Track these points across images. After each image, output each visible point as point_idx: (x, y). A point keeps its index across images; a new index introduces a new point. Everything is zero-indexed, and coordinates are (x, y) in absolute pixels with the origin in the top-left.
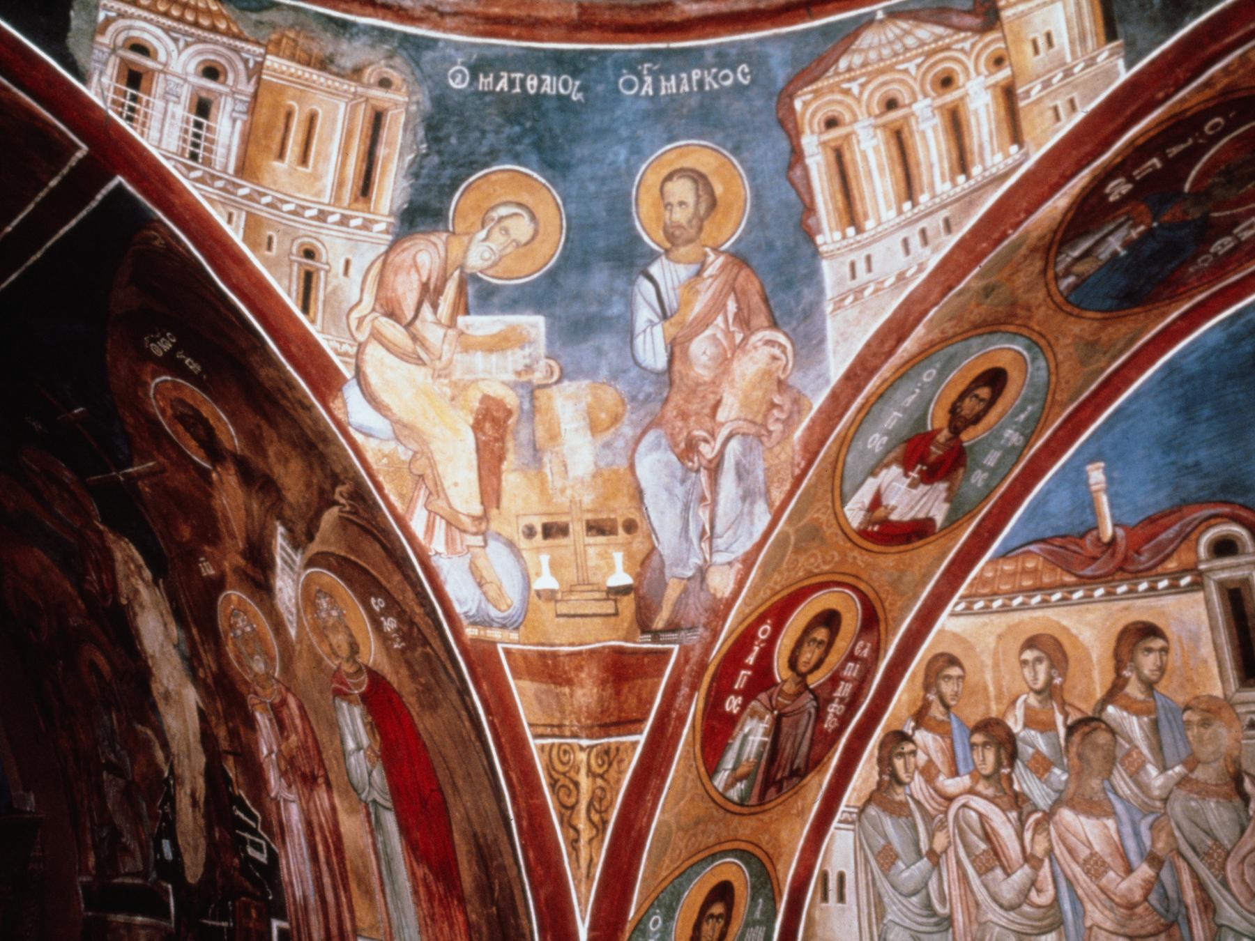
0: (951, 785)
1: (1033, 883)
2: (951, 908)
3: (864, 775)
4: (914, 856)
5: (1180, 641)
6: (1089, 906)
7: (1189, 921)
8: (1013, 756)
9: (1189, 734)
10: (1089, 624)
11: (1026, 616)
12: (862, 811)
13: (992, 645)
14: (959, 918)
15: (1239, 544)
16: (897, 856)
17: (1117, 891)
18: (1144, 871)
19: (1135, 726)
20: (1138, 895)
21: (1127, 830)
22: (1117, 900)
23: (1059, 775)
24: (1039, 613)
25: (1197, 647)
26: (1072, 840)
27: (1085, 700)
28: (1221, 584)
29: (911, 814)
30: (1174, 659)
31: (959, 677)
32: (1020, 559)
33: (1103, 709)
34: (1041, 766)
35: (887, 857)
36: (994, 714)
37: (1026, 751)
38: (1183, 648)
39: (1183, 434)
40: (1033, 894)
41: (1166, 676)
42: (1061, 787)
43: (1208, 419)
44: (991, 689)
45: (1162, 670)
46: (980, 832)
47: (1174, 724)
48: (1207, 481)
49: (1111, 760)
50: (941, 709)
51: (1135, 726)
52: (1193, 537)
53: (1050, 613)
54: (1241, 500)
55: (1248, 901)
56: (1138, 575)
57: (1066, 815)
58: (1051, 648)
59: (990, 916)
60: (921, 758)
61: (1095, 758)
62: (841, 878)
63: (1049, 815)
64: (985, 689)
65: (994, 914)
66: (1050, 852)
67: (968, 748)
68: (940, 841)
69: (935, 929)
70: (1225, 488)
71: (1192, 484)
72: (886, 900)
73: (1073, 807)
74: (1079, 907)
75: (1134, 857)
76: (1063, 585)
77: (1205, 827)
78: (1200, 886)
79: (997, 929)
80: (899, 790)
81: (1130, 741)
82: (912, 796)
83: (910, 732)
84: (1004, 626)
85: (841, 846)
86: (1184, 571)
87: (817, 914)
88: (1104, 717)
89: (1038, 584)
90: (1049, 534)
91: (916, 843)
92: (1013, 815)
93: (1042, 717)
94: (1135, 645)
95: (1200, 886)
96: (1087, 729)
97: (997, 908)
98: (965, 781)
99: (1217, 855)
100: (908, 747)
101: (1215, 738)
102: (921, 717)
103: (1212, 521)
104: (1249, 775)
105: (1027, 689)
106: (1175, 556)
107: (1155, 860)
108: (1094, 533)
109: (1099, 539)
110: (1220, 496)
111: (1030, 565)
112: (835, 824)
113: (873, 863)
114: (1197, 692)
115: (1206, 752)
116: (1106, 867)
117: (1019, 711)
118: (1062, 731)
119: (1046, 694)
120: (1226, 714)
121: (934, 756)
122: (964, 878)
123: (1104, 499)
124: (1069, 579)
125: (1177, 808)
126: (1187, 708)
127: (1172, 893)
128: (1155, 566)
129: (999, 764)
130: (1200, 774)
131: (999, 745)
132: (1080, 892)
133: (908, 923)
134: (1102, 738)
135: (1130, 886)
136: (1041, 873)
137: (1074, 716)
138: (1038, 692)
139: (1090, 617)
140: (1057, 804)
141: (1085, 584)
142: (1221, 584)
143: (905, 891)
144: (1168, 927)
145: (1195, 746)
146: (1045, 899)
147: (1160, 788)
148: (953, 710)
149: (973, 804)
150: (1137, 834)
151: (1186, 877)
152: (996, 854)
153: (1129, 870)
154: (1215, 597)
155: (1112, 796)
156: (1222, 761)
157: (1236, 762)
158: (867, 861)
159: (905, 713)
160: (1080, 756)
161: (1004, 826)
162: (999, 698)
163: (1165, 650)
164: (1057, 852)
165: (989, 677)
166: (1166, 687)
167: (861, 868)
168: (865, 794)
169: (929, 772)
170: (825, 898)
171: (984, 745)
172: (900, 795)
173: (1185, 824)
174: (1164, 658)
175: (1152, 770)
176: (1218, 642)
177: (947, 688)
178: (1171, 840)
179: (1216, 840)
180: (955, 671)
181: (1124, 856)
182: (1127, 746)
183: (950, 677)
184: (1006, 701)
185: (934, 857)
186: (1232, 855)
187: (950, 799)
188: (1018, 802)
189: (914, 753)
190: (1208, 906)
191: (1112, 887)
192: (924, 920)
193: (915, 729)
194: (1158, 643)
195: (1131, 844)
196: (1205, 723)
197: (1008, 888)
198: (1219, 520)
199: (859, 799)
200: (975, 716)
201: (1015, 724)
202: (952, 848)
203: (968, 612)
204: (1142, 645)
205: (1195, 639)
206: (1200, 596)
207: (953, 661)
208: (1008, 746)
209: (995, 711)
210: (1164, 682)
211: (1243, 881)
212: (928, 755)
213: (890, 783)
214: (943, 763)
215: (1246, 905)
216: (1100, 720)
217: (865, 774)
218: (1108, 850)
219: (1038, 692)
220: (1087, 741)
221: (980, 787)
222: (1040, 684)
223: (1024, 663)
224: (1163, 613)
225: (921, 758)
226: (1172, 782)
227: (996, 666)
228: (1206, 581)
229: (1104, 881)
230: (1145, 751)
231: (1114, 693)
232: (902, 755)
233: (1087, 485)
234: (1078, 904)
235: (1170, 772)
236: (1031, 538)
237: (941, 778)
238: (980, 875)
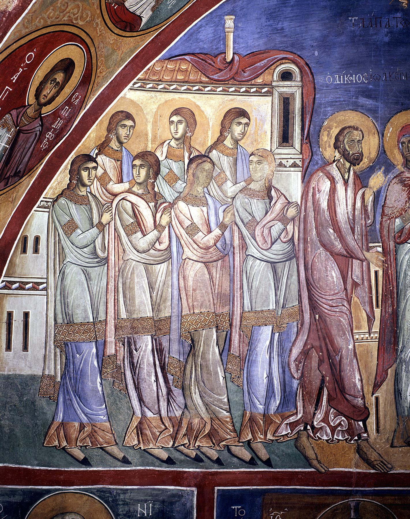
0: (117, 188)
1: (158, 239)
2: (108, 253)
3: (59, 180)
4: (88, 226)
5: (256, 119)
6: (186, 249)
7: (234, 254)
8: (157, 173)
9: (251, 167)
10: (211, 106)
11: (177, 96)
12: (56, 200)
13: (155, 110)
14: (112, 258)
15: (293, 75)
16: (77, 227)
17: (202, 242)
18: (217, 232)
19: (225, 162)
20: (212, 243)
21: (212, 212)
22: (201, 246)
23: (180, 185)
24: (184, 96)
25: (263, 125)
26: (182, 217)
27: (203, 146)
28: (281, 94)
29: (88, 204)
30: (251, 129)
31: (131, 126)
32: (179, 62)
33: (210, 151)
34: (172, 179)
35: (71, 227)
36: (149, 150)
37: (164, 171)
38: (256, 124)
39: (279, 11)
40: (157, 245)
41: (245, 137)
42: (181, 191)
43: (292, 6)
44: (150, 135)
45: (244, 134)
46: (131, 213)
47: (244, 162)
48: (285, 39)
49: (210, 177)
50: (117, 144)
51: (225, 162)
52: (273, 67)
53: (190, 96)
54: (299, 53)
55: (262, 245)
56: (241, 83)
57: (181, 205)
58: (187, 116)
59: (131, 257)
60: (100, 171)
61: (202, 176)
62: (37, 239)
63: (172, 205)
64: (147, 135)
65: (132, 255)
66: (170, 224)
67: (130, 167)
68: (106, 218)
69: (97, 265)
70: (292, 45)
71: (278, 39)
72: (67, 251)
73: (185, 200)
74: (181, 250)
75: (213, 225)
76: (201, 82)
77: (250, 211)
78: (242, 237)
79: (134, 262)
80: (83, 189)
81: (222, 169)
82: (91, 193)
83: (94, 156)
84: (163, 101)
85: (38, 222)
86: (265, 85)
87: (18, 261)
88: (210, 156)
89: (186, 79)
90: (197, 51)
91: (91, 219)
92: (152, 204)
93: (177, 152)
94: (234, 119)
95: (242, 237)
96: (200, 161)
97: (136, 252)
98: (126, 186)
99: (252, 224)
100: (92, 165)
101: (262, 169)
102: (102, 148)
103: (284, 61)
104: (274, 187)
105: (171, 138)
106: (262, 76)
107: (223, 227)
108: (223, 55)
109: (225, 59)
110: (289, 49)
111: (184, 67)
112: (35, 208)
113: (61, 231)
114: (259, 147)
115: (257, 176)
116: (198, 230)
117: (165, 149)
118: (187, 161)
119: (181, 141)
120: (270, 158)
121: (108, 171)
122: (118, 237)
123: (231, 36)
124: (204, 79)
125: (238, 203)
126: (252, 154)
127: (228, 242)
128: (251, 80)
129: (148, 176)
130: (252, 186)
131: (150, 167)
132: (182, 242)
133: (80, 262)
134: (207, 166)
135: (210, 239)
136: (163, 234)
137: (195, 154)
138: (177, 139)
139: (212, 102)
140: (177, 199)
141: (212, 83)
142: (281, 94)
143: (80, 245)
144: (222, 258)
145: (252, 172)
146: (163, 246)
147: (231, 192)
148: (123, 145)
149: (128, 198)
150: (217, 214)
151: (236, 234)
152: (139, 224)
153: (210, 231)
154: (276, 101)
155: (207, 195)
156: (264, 180)
157: (270, 181)
158: (56, 228)
159: (92, 145)
160: (194, 175)
161: (145, 211)
162: (154, 140)
163: (247, 124)
164: (173, 223)
165: (149, 128)
166: (244, 143)
167: (52, 234)
168: (58, 191)
169: (104, 180)
170: (24, 251)
171: (141, 166)
172: (83, 191)
173: (241, 210)
174: (246, 128)
175: (229, 184)
176: (274, 123)
177: (123, 132)
178: (233, 216)
179: (254, 217)
180: (129, 123)
181: (208, 225)
182: (219, 171)
183: (125, 126)
184: (157, 143)
185: (101, 227)
186: (260, 224)
187: (116, 195)
188: (155, 198)
189: (95, 168)
190: (244, 246)
191: (200, 240)
192: (90, 260)
193: (97, 155)
194: (244, 120)
195: (213, 219)
196: (259, 162)
197: (143, 242)
198: (287, 61)
199: (54, 194)
200: (136, 148)
201: (161, 155)
202: (113, 222)
203: (142, 88)
204: (237, 120)
205: (263, 121)
206: (270, 98)
207: (129, 116)
208: (155, 167)
209: (150, 148)
210: (243, 141)
211: (262, 235)
212: (105, 170)
213: (77, 185)
214: (114, 175)
215: (261, 246)
216: (208, 157)
217: (61, 179)
218: (200, 222)
219: (177, 139)
220: (199, 167)
221: (135, 189)
222: (178, 136)
223: (172, 122)
224: (250, 106)
225: (100, 171)
226: (239, 189)
227: (155, 123)
228: (274, 91)
229: (196, 237)
230: (228, 173)
231: (217, 144)
232: (87, 169)
233: (224, 27)
234: (181, 250)
235: (238, 185)
236: (187, 51)
237: (111, 183)
238: (128, 236)
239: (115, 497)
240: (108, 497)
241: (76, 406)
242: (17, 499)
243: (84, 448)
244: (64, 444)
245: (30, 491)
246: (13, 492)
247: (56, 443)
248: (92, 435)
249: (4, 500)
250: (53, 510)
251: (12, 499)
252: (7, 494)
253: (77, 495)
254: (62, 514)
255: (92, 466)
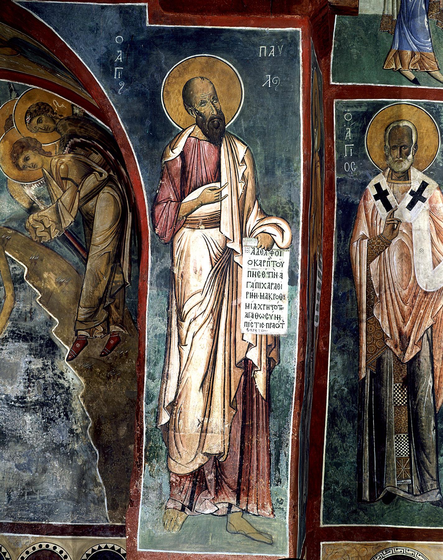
239: (438, 109)
240: (433, 109)
241: (409, 38)
242: (363, 109)
243: (414, 71)
244: (400, 67)
245: (373, 103)
246: (360, 104)
247: (394, 66)
248: (420, 62)
249: (353, 110)
250: (390, 118)
251: (359, 110)
252: (355, 106)
253: (410, 107)
254: (398, 121)
255: (420, 85)
